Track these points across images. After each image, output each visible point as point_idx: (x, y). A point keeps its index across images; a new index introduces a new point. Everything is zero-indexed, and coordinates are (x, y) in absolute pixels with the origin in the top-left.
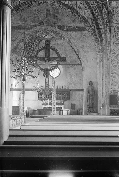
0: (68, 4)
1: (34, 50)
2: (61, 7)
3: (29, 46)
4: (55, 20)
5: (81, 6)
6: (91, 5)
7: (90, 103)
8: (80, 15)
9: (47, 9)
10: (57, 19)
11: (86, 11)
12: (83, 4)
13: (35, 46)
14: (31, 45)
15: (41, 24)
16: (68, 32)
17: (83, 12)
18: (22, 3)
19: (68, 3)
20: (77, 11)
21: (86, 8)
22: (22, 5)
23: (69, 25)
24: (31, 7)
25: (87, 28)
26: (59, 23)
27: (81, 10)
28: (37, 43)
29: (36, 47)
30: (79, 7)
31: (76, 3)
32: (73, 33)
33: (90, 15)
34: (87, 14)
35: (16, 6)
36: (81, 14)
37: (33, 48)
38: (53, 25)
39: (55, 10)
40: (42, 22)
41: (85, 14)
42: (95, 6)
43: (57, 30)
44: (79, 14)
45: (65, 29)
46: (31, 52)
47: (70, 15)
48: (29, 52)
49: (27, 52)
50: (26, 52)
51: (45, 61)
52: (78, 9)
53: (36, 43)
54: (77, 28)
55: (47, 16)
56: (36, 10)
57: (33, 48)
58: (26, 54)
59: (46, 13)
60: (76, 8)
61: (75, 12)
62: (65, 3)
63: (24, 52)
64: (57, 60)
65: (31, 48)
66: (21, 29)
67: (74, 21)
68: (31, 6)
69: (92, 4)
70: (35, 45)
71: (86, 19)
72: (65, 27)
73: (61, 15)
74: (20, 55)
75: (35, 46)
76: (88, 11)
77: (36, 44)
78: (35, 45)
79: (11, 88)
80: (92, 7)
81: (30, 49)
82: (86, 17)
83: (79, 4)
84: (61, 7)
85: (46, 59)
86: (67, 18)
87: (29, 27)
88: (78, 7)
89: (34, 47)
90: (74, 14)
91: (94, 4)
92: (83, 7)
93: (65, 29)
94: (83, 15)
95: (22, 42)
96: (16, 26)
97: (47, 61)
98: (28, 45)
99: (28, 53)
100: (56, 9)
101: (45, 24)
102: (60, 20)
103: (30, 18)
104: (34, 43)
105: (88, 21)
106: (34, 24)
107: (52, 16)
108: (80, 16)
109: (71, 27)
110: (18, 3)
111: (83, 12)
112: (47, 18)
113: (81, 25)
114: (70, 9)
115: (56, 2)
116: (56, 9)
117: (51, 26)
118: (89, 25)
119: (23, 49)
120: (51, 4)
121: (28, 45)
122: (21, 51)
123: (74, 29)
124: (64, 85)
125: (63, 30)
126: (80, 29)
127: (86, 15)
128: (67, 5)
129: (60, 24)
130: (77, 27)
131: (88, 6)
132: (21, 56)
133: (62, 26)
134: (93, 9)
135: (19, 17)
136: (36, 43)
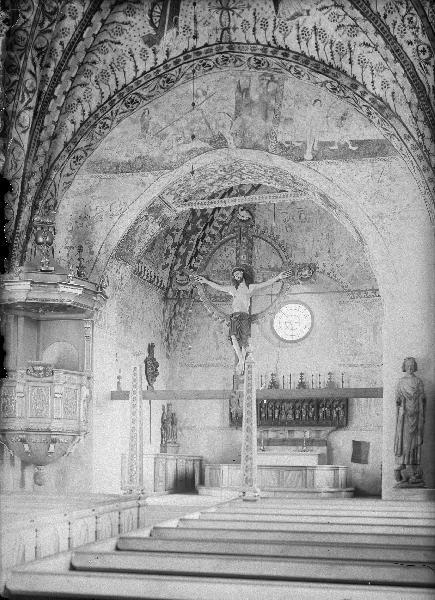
0: (315, 54)
2: (292, 70)
4: (270, 124)
5: (368, 57)
6: (405, 45)
7: (405, 446)
8: (365, 93)
9: (239, 88)
10: (277, 120)
11: (388, 75)
12: (376, 48)
13: (216, 228)
15: (218, 142)
16: (323, 166)
17: (378, 84)
18: (144, 73)
19: (317, 50)
20: (354, 78)
21: (386, 60)
22: (144, 81)
23: (327, 138)
24: (180, 82)
25: (395, 142)
26: (284, 134)
27: (368, 71)
28: (223, 216)
30: (362, 62)
31: (346, 46)
32: (336, 169)
33: (403, 89)
34: (393, 86)
35: (125, 86)
36: (369, 87)
37: (213, 236)
38: (262, 143)
39: (271, 84)
40: (221, 137)
41: (385, 85)
42: (421, 48)
43: (278, 161)
44: (361, 89)
45: (308, 156)
47: (326, 96)
48: (197, 252)
50: (186, 254)
51: (237, 284)
52: (356, 70)
53: (221, 219)
54: (354, 149)
55: (238, 113)
56: (200, 92)
57: (213, 236)
59: (233, 101)
60: (346, 67)
61: (345, 83)
62: (306, 51)
64: (280, 277)
65: (204, 235)
66: (143, 168)
67: (342, 118)
68: (178, 79)
69: (410, 43)
71: (388, 106)
72: (309, 150)
73: (291, 102)
74: (164, 268)
75: (216, 228)
76: (395, 74)
77: (220, 223)
79: (115, 389)
80: (410, 54)
81: (198, 240)
82: (390, 100)
83: (358, 51)
84: (292, 70)
85: (238, 275)
86: (313, 111)
87: (174, 159)
88: (355, 61)
89: (214, 232)
90: (342, 94)
91: (419, 42)
92: (375, 58)
93: (308, 156)
94: (379, 91)
95: (151, 218)
96: (127, 160)
97: (243, 284)
98: (190, 228)
99: (191, 259)
100: (272, 79)
101: (230, 142)
102: (289, 120)
103: (178, 125)
104: (213, 220)
105: (398, 117)
106: (189, 147)
107: (255, 110)
108: (367, 98)
109: (332, 144)
110: (131, 74)
111: (378, 84)
112: (239, 121)
113: (373, 133)
114: (325, 73)
115: (269, 53)
116: (272, 79)
117: (256, 147)
118: (402, 131)
119: (174, 245)
120: (253, 62)
121: (190, 228)
122: (168, 251)
123: (344, 154)
124: (324, 371)
125: (302, 160)
126: (366, 150)
127: (389, 93)
128: (313, 58)
129: (289, 139)
130: (354, 143)
131: (392, 51)
132: (168, 270)
133: (297, 144)
134: (416, 64)
135: (138, 126)
136: (221, 219)
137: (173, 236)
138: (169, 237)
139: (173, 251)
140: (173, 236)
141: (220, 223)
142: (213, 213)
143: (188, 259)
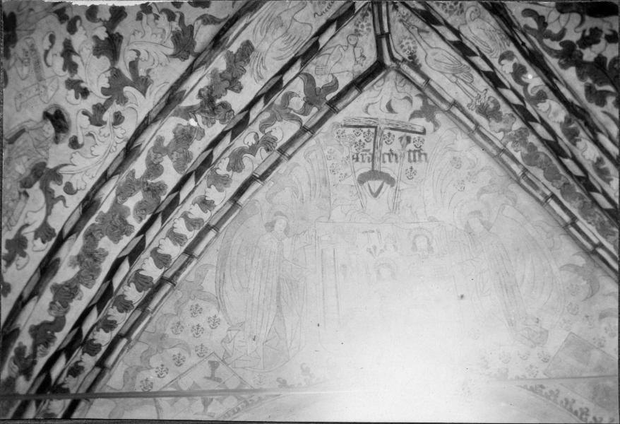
1: (163, 281)
3: (117, 226)
13: (177, 238)
14: (141, 207)
29: (189, 252)
46: (125, 306)
48: (106, 294)
49: (88, 293)
53: (196, 212)
57: (162, 260)
58: (72, 317)
63: (48, 267)
70: (181, 227)
75: (177, 238)
77: (191, 223)
78: (181, 227)
104: (174, 204)
119: (44, 231)
136: (196, 212)
137: (51, 200)
138: (36, 191)
139: (37, 250)
140: (51, 200)
141: (191, 223)
142: (178, 188)
143: (77, 308)
